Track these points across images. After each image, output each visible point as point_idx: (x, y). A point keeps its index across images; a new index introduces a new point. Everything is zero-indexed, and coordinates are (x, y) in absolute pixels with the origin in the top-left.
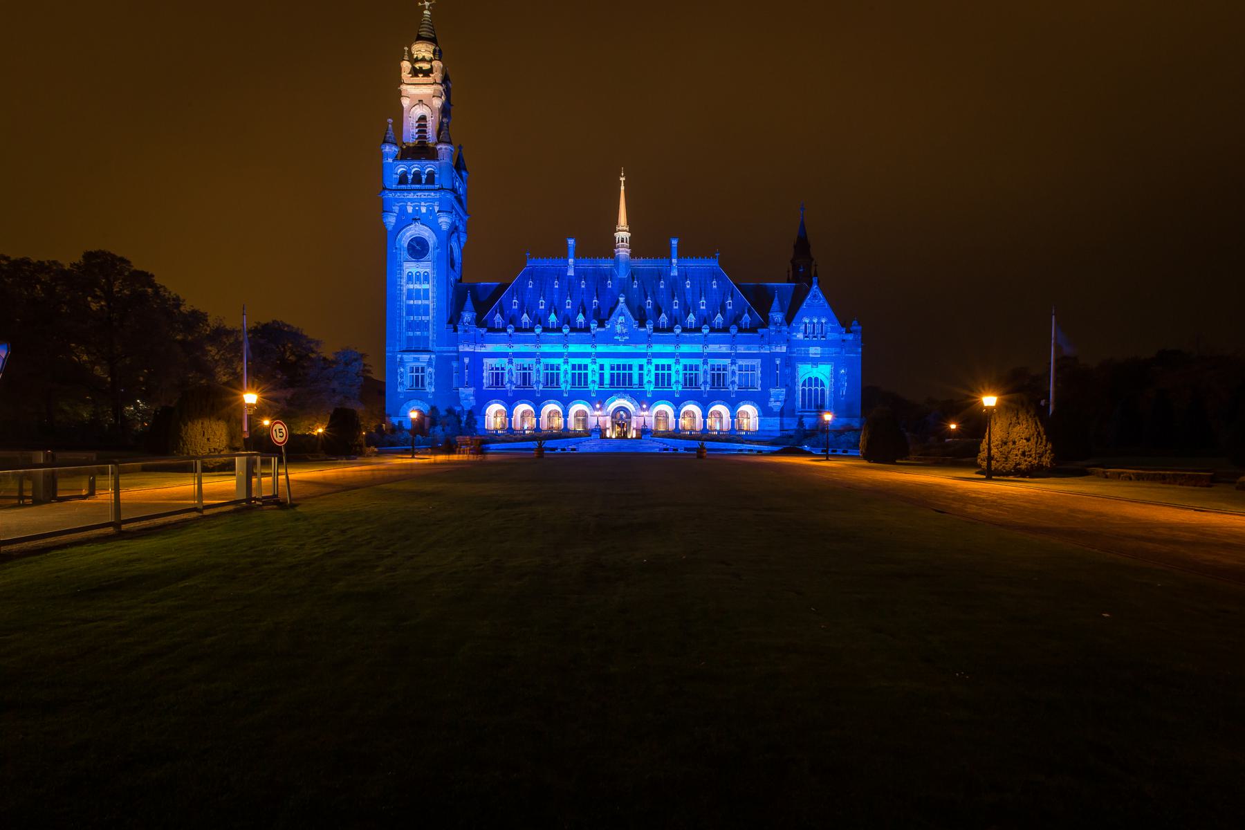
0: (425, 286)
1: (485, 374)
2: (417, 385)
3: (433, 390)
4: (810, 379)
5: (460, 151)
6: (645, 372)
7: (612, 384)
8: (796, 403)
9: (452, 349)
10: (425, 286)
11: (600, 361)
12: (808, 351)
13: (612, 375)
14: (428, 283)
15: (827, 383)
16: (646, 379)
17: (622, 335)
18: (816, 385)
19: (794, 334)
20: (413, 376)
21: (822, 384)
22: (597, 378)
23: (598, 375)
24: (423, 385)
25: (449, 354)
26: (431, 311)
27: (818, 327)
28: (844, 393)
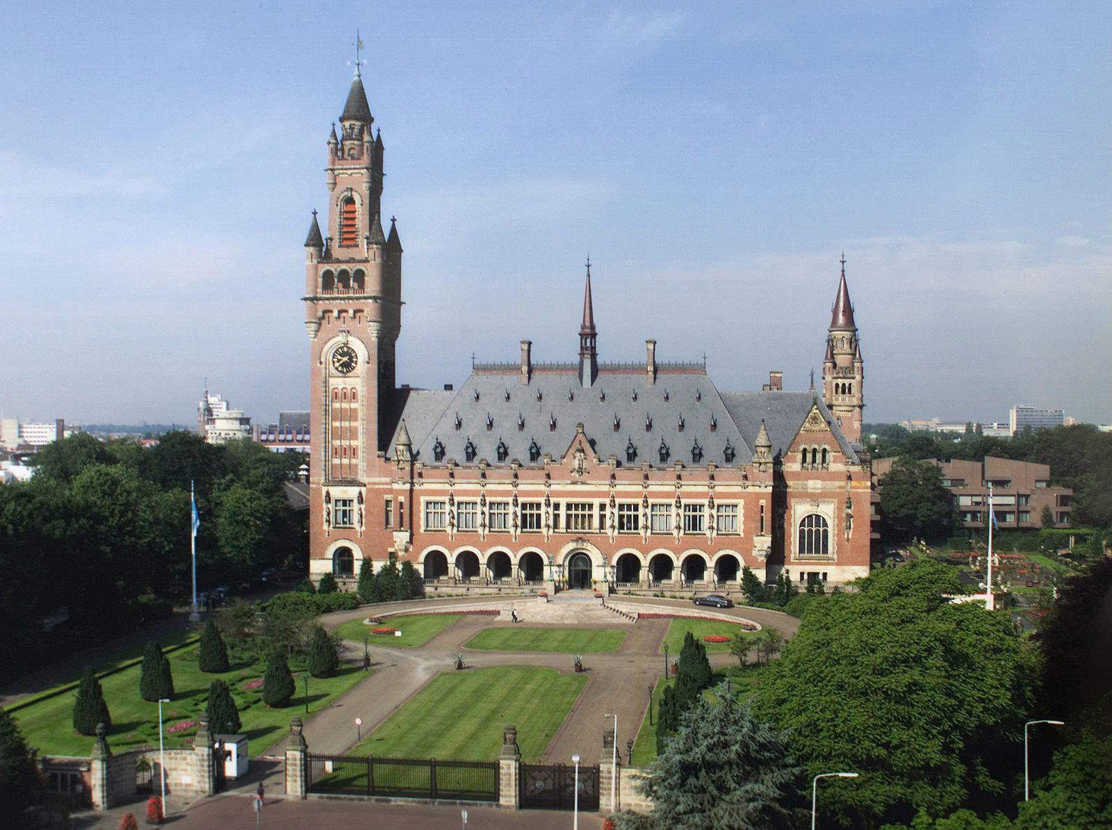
0: (354, 405)
3: (363, 528)
4: (810, 517)
5: (394, 225)
6: (608, 512)
7: (568, 526)
8: (792, 549)
9: (384, 480)
10: (354, 405)
12: (806, 485)
13: (569, 516)
14: (357, 402)
15: (830, 522)
16: (608, 523)
18: (818, 525)
19: (789, 464)
21: (825, 525)
22: (551, 522)
23: (551, 518)
25: (381, 486)
26: (360, 436)
27: (819, 457)
28: (850, 536)
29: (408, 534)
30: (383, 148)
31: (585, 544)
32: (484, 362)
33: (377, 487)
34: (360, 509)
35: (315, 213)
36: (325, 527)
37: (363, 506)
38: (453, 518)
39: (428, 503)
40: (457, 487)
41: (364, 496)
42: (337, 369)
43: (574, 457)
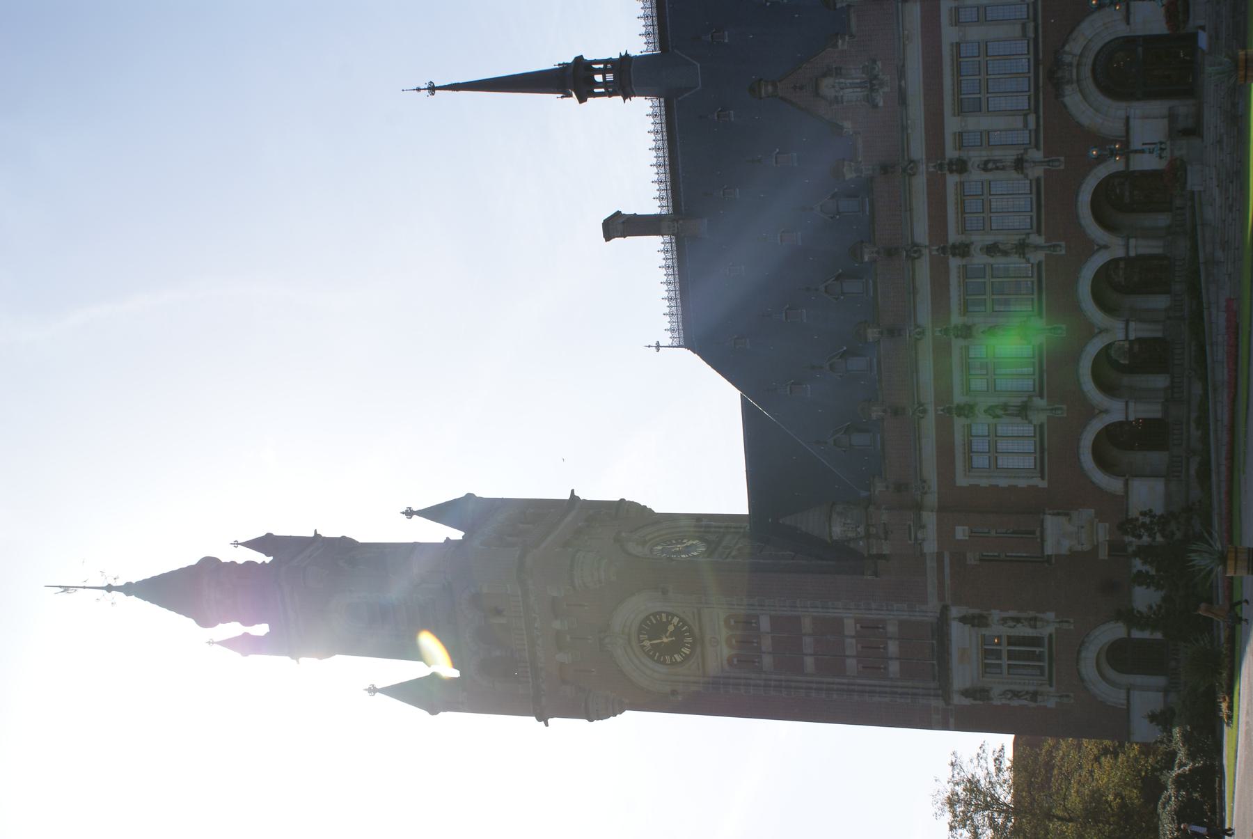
1: (1003, 483)
2: (1039, 657)
3: (1050, 616)
9: (931, 564)
11: (951, 153)
17: (871, 84)
20: (1009, 666)
24: (1036, 641)
25: (947, 570)
29: (1050, 522)
30: (269, 535)
31: (1067, 59)
32: (665, 322)
33: (948, 581)
34: (1004, 621)
35: (373, 690)
36: (1051, 703)
37: (996, 615)
38: (1005, 407)
39: (970, 467)
40: (928, 393)
41: (976, 611)
42: (687, 658)
43: (837, 100)
